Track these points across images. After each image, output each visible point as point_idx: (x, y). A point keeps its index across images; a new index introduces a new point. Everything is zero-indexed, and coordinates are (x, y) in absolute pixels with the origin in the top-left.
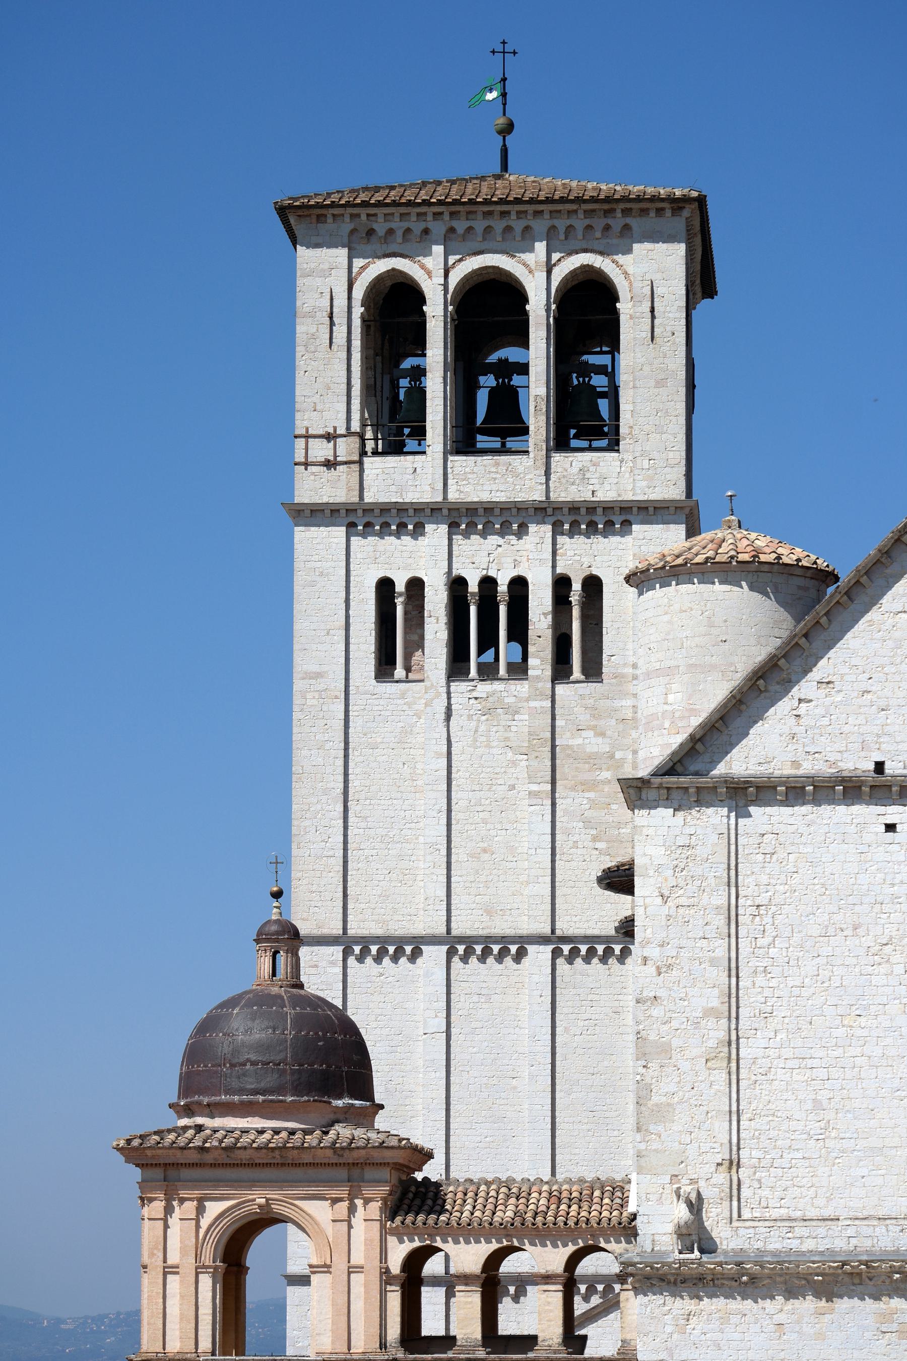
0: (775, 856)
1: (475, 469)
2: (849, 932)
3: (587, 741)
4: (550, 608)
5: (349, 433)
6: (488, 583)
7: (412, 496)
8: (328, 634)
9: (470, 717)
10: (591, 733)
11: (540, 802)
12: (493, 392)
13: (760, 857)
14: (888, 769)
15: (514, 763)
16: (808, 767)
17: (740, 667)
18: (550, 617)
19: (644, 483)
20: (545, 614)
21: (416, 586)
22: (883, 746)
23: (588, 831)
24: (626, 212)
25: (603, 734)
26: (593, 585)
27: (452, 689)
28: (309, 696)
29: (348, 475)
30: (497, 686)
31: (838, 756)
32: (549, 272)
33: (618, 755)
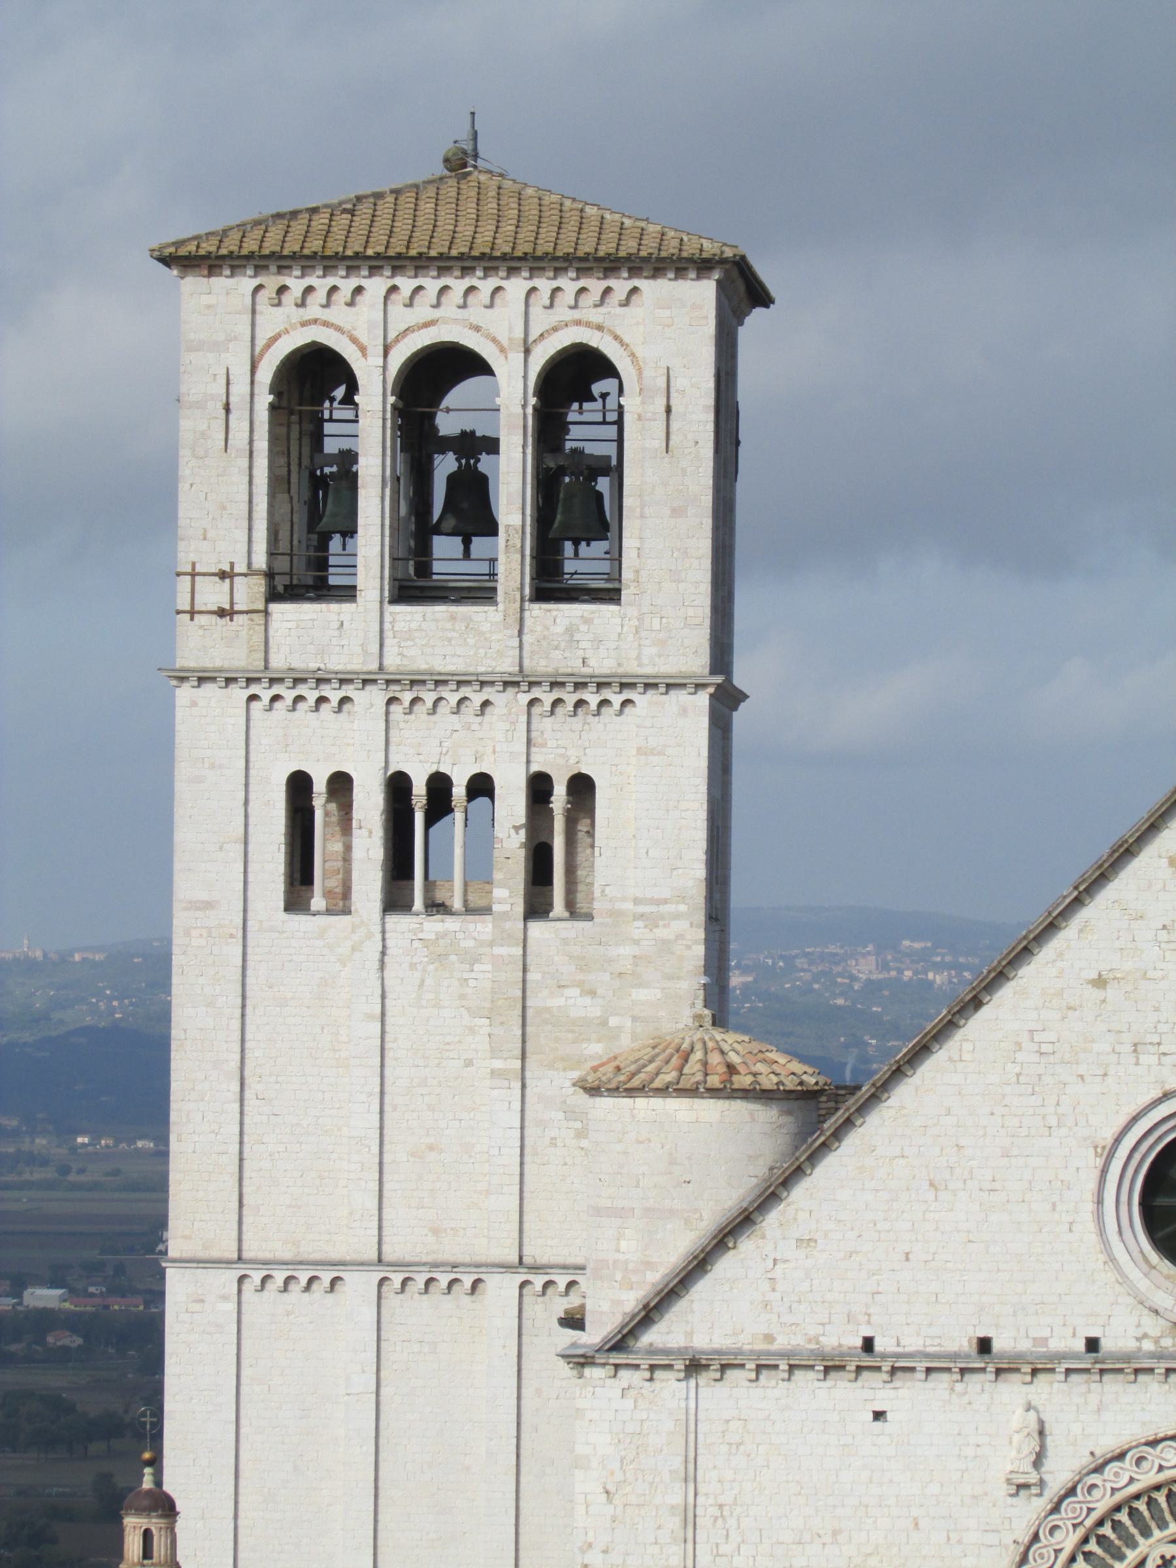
0: (742, 1448)
1: (424, 626)
2: (828, 1539)
3: (571, 1002)
4: (523, 820)
5: (251, 572)
6: (439, 785)
7: (336, 663)
8: (221, 849)
9: (413, 966)
10: (575, 992)
11: (506, 1083)
12: (452, 479)
13: (724, 1448)
14: (879, 1346)
15: (472, 1030)
16: (782, 1342)
17: (706, 1215)
18: (523, 832)
19: (654, 650)
20: (517, 828)
21: (341, 784)
22: (873, 1318)
23: (571, 1124)
24: (635, 272)
25: (592, 993)
26: (581, 787)
27: (388, 926)
28: (194, 933)
29: (250, 629)
30: (450, 924)
31: (820, 1330)
32: (527, 352)
33: (613, 1021)
